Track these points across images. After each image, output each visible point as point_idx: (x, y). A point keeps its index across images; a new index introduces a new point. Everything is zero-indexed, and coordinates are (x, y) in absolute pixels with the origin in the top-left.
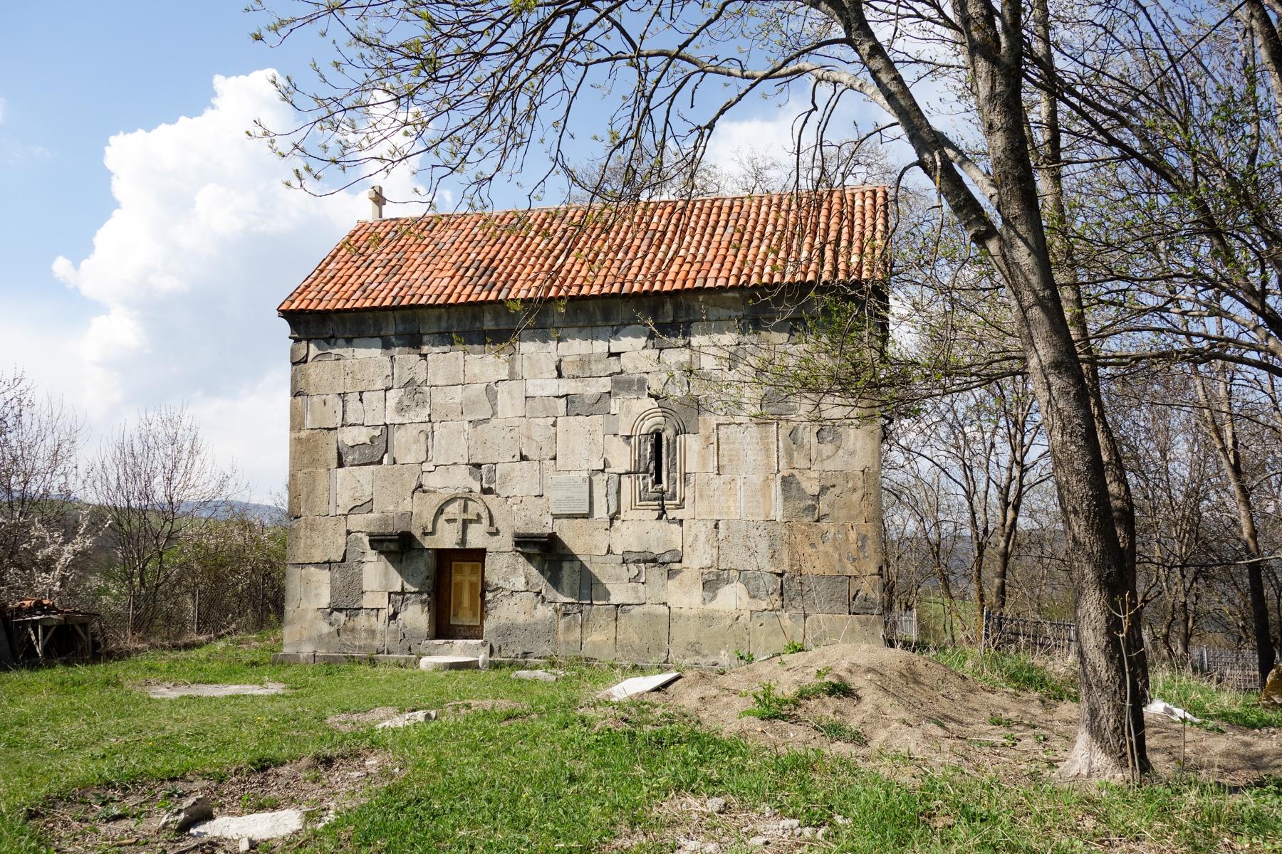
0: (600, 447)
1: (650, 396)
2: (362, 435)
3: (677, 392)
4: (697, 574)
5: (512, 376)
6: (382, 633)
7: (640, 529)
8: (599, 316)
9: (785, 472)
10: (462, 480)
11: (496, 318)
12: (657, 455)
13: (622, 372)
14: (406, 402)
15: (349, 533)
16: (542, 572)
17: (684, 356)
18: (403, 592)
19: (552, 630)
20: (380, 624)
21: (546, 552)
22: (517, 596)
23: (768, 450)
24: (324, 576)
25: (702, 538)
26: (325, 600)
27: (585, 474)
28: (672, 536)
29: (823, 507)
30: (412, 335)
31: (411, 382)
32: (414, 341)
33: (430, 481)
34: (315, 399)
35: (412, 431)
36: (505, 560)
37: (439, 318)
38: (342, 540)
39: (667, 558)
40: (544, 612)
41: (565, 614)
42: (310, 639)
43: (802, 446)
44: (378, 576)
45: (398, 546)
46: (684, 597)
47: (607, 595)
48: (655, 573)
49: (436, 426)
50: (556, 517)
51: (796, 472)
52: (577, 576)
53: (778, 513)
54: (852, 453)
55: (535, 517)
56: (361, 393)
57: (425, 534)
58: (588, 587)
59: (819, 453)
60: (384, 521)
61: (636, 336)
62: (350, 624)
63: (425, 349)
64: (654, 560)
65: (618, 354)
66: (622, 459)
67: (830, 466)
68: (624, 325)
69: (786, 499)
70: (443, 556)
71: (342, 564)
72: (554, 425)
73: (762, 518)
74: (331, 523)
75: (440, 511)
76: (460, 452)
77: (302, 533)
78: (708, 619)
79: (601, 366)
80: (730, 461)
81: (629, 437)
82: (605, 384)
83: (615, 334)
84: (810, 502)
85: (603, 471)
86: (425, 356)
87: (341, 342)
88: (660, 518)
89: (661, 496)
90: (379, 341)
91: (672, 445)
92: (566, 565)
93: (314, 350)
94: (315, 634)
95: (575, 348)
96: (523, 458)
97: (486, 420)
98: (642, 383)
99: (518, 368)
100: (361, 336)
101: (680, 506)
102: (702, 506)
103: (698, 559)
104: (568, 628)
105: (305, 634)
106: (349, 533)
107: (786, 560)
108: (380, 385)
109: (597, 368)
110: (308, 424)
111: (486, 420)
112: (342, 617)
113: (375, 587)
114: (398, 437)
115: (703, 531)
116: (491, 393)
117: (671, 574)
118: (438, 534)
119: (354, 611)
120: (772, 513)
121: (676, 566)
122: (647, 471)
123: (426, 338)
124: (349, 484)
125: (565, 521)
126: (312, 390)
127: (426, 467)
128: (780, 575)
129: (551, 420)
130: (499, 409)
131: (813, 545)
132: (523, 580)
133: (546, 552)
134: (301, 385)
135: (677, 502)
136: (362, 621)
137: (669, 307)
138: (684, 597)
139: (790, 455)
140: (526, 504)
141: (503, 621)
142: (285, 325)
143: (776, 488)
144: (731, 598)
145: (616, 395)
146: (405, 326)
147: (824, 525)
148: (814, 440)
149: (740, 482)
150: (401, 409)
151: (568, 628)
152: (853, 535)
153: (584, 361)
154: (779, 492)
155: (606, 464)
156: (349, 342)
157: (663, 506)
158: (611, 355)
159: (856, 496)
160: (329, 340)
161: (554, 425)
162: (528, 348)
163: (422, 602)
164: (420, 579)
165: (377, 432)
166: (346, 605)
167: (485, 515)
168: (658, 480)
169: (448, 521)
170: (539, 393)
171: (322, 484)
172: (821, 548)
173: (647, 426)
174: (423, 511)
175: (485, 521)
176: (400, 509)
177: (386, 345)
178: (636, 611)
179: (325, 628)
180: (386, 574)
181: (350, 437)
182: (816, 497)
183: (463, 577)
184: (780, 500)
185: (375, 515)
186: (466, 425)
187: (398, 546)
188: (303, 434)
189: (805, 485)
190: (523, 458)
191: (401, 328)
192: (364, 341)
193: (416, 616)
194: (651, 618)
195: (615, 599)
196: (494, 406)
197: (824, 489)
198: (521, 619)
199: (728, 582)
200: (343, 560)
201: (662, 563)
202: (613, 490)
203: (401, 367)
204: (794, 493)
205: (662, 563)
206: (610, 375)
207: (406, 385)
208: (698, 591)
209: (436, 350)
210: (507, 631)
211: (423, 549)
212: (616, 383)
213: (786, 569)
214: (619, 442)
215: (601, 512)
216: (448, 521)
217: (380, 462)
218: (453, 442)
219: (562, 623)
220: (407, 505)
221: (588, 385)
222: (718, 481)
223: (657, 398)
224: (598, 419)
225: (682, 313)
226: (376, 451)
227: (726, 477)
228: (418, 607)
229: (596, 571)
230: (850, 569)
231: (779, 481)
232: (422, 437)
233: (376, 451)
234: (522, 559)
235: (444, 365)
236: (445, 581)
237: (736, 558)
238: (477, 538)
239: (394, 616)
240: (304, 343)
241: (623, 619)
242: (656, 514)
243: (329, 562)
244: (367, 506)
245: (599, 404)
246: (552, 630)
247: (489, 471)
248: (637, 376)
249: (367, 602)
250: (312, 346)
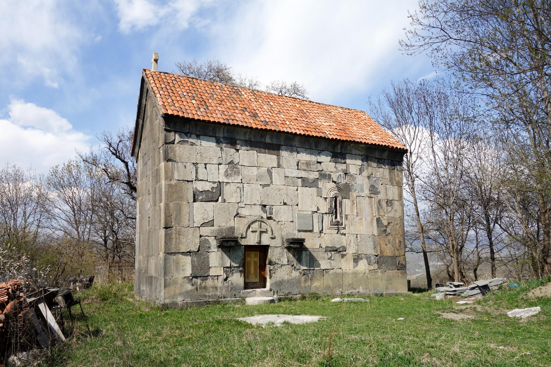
0: (311, 201)
1: (333, 181)
2: (207, 186)
3: (343, 182)
4: (351, 256)
5: (279, 166)
6: (220, 288)
7: (330, 238)
8: (313, 145)
9: (378, 217)
10: (257, 212)
11: (271, 138)
13: (322, 170)
14: (229, 172)
15: (201, 236)
16: (294, 256)
17: (344, 167)
18: (230, 267)
19: (299, 282)
20: (219, 283)
22: (284, 267)
23: (372, 207)
24: (188, 260)
25: (352, 241)
26: (188, 272)
27: (310, 213)
28: (344, 241)
29: (388, 230)
30: (231, 139)
31: (231, 162)
32: (232, 143)
33: (243, 212)
34: (179, 164)
35: (233, 187)
36: (278, 250)
37: (245, 133)
38: (197, 240)
39: (341, 249)
40: (295, 274)
41: (304, 275)
42: (180, 294)
43: (382, 207)
44: (217, 260)
45: (229, 244)
46: (347, 265)
47: (319, 265)
48: (337, 256)
49: (245, 185)
51: (380, 217)
52: (308, 258)
53: (376, 233)
54: (396, 211)
55: (291, 231)
56: (206, 164)
57: (242, 238)
58: (312, 262)
59: (387, 210)
60: (220, 231)
61: (327, 156)
62: (203, 285)
63: (238, 147)
64: (336, 251)
65: (320, 163)
66: (325, 207)
67: (391, 215)
68: (323, 151)
69: (378, 227)
70: (249, 248)
71: (199, 254)
73: (371, 234)
74: (191, 230)
75: (249, 227)
76: (257, 199)
77: (174, 236)
78: (355, 274)
79: (315, 167)
81: (326, 198)
82: (316, 175)
83: (319, 154)
84: (385, 228)
85: (316, 212)
86: (238, 150)
87: (193, 136)
89: (338, 224)
90: (214, 139)
91: (341, 203)
92: (304, 253)
93: (178, 138)
94: (183, 290)
95: (304, 157)
96: (285, 204)
97: (268, 185)
98: (330, 176)
99: (281, 163)
100: (205, 135)
101: (344, 228)
102: (352, 228)
104: (306, 281)
105: (177, 292)
106: (201, 236)
107: (379, 250)
108: (215, 161)
109: (313, 167)
110: (176, 177)
111: (268, 185)
112: (199, 281)
113: (217, 265)
114: (227, 190)
115: (353, 238)
116: (269, 172)
117: (343, 256)
118: (248, 238)
119: (205, 277)
121: (344, 253)
123: (238, 142)
124: (201, 211)
125: (302, 233)
126: (177, 159)
127: (240, 205)
128: (377, 256)
129: (296, 188)
130: (273, 180)
131: (386, 245)
132: (286, 260)
133: (297, 247)
134: (171, 156)
135: (343, 226)
136: (209, 282)
137: (339, 146)
138: (347, 265)
139: (378, 210)
140: (286, 225)
141: (278, 279)
144: (363, 265)
145: (320, 180)
147: (389, 237)
148: (385, 205)
149: (364, 219)
150: (227, 175)
151: (306, 281)
152: (397, 241)
153: (308, 164)
155: (318, 209)
156: (198, 137)
158: (318, 162)
160: (188, 134)
161: (297, 190)
162: (284, 154)
163: (241, 271)
164: (239, 260)
165: (215, 185)
166: (200, 273)
167: (269, 229)
168: (336, 218)
169: (253, 232)
170: (290, 175)
171: (185, 209)
172: (388, 245)
173: (332, 194)
174: (240, 227)
175: (270, 232)
176: (228, 225)
177: (218, 142)
178: (331, 272)
179: (189, 287)
180: (222, 258)
181: (200, 186)
182: (386, 226)
184: (376, 227)
185: (215, 228)
186: (259, 186)
187: (229, 244)
188: (173, 182)
189: (383, 221)
190: (285, 204)
191: (226, 135)
192: (206, 138)
193: (237, 279)
194: (337, 274)
195: (322, 267)
196: (271, 178)
197: (389, 223)
198: (286, 277)
199: (361, 259)
200: (198, 251)
201: (339, 251)
202: (321, 221)
203: (227, 154)
204: (380, 224)
205: (339, 251)
206: (318, 171)
207: (229, 163)
208: (352, 263)
209: (244, 148)
210: (279, 284)
211: (241, 245)
212: (320, 175)
213: (379, 253)
214: (322, 200)
215: (316, 230)
216: (253, 232)
217: (217, 201)
218: (254, 194)
219: (303, 278)
220: (231, 224)
221: (310, 174)
222: (357, 219)
223: (335, 182)
224: (315, 189)
225: (343, 150)
226: (214, 195)
227: (359, 217)
228: (239, 274)
229: (315, 255)
230: (397, 253)
231: (375, 220)
232: (238, 190)
233: (214, 195)
234: (285, 250)
235: (245, 156)
236: (252, 260)
238: (266, 240)
239: (226, 280)
240: (173, 133)
241: (326, 276)
242: (337, 231)
243: (190, 252)
244: (211, 223)
245: (313, 184)
246: (299, 282)
247: (270, 208)
248: (328, 173)
249: (212, 272)
250: (177, 136)
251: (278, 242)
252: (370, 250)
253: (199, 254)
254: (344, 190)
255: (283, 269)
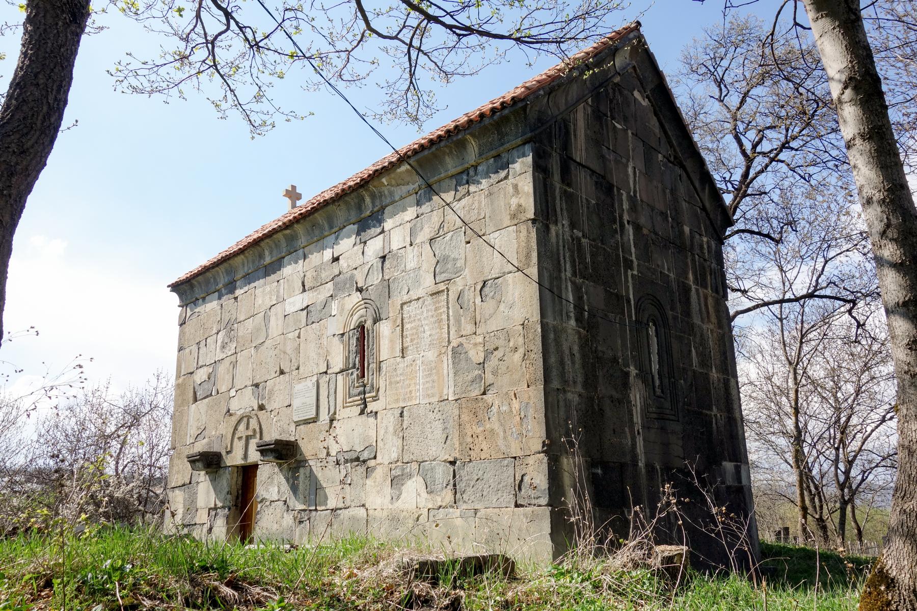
25: (391, 429)
50: (298, 424)
61: (349, 236)
72: (299, 337)
73: (435, 400)
78: (395, 520)
80: (412, 340)
81: (343, 335)
84: (477, 372)
85: (326, 373)
88: (362, 413)
92: (302, 470)
118: (234, 452)
120: (445, 392)
122: (354, 367)
128: (453, 463)
142: (175, 298)
143: (447, 364)
154: (451, 366)
157: (365, 399)
159: (518, 356)
161: (299, 337)
189: (472, 353)
190: (282, 372)
197: (488, 354)
199: (410, 476)
200: (190, 483)
204: (463, 363)
213: (457, 455)
217: (211, 395)
222: (402, 364)
242: (358, 410)
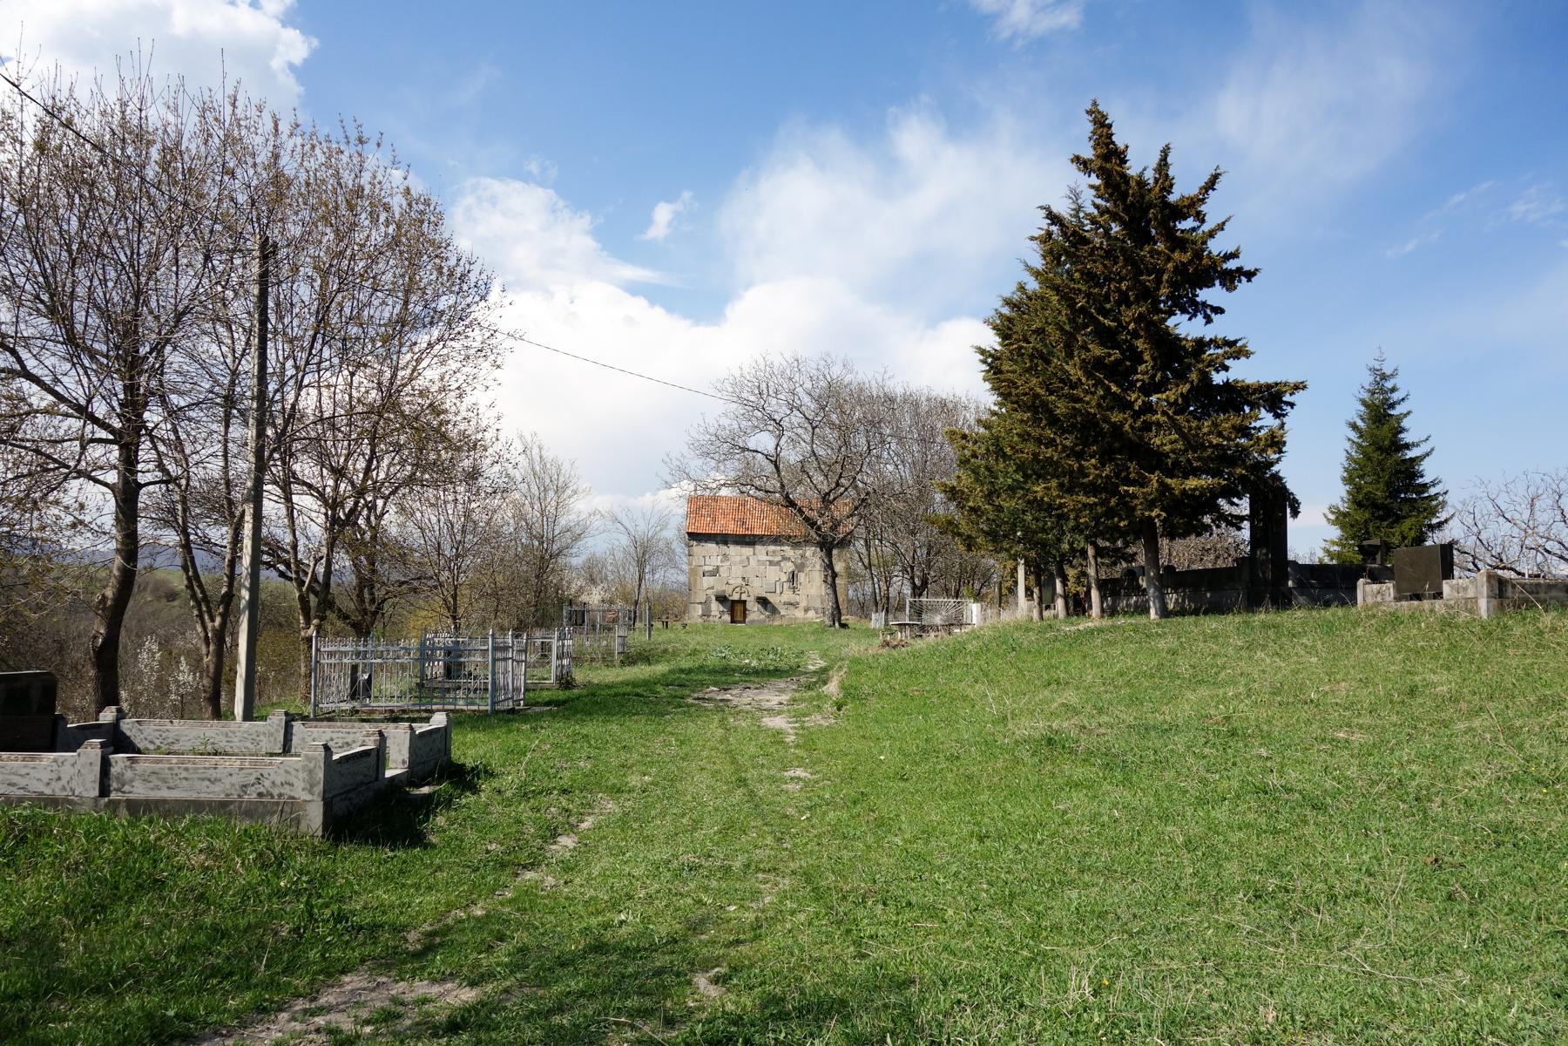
0: (776, 575)
7: (788, 596)
10: (740, 581)
12: (793, 577)
21: (763, 602)
32: (726, 543)
44: (715, 607)
45: (722, 599)
46: (799, 614)
58: (774, 611)
66: (784, 578)
71: (706, 604)
95: (772, 548)
103: (803, 604)
124: (707, 581)
133: (763, 602)
138: (799, 614)
140: (757, 588)
144: (811, 614)
146: (723, 539)
166: (706, 614)
174: (728, 590)
181: (706, 568)
183: (739, 608)
187: (722, 599)
193: (727, 618)
201: (794, 605)
205: (794, 605)
218: (738, 571)
233: (715, 573)
235: (733, 550)
236: (735, 608)
237: (812, 604)
238: (744, 597)
245: (778, 563)
251: (752, 598)
252: (818, 604)
253: (706, 604)
254: (800, 567)
255: (755, 612)
